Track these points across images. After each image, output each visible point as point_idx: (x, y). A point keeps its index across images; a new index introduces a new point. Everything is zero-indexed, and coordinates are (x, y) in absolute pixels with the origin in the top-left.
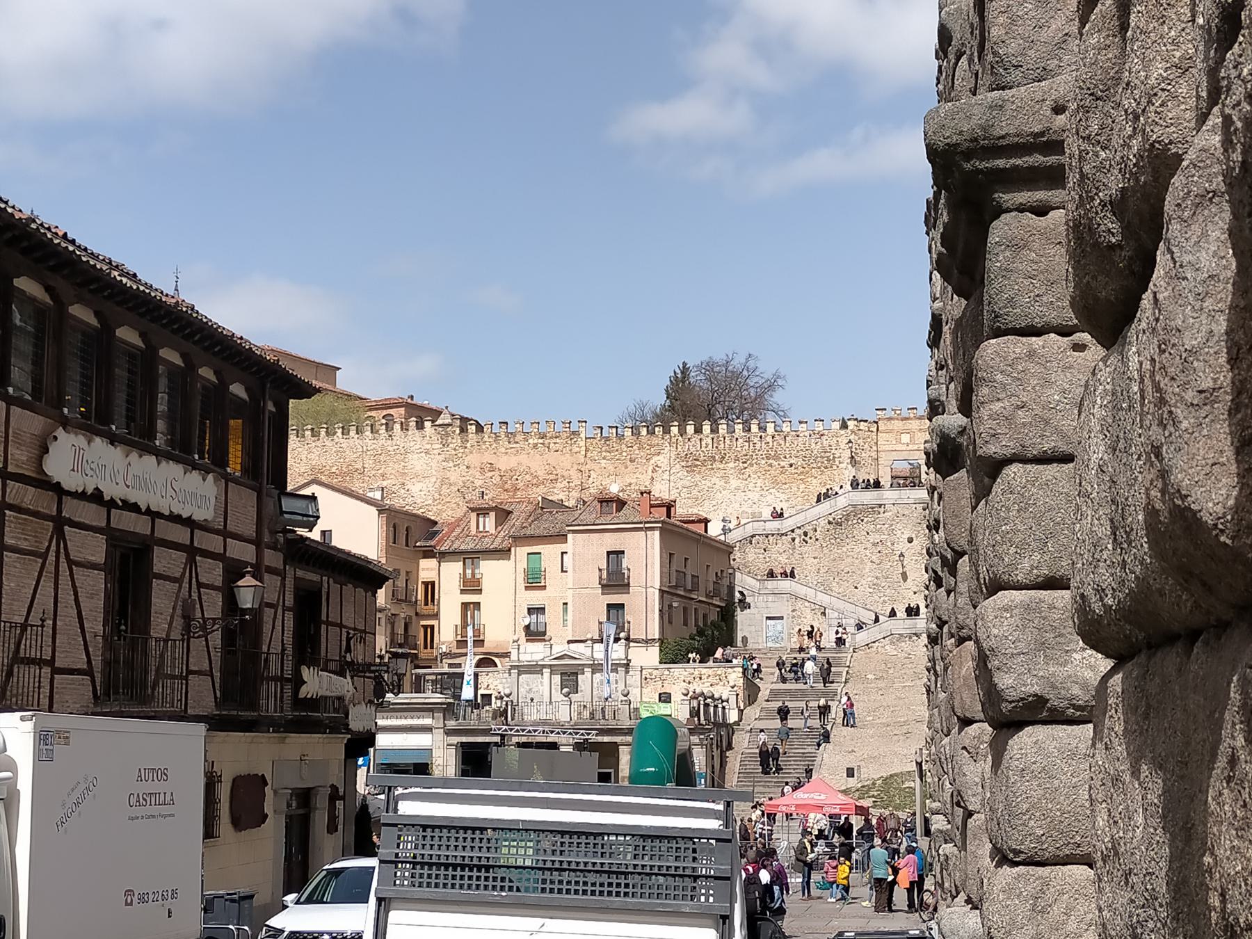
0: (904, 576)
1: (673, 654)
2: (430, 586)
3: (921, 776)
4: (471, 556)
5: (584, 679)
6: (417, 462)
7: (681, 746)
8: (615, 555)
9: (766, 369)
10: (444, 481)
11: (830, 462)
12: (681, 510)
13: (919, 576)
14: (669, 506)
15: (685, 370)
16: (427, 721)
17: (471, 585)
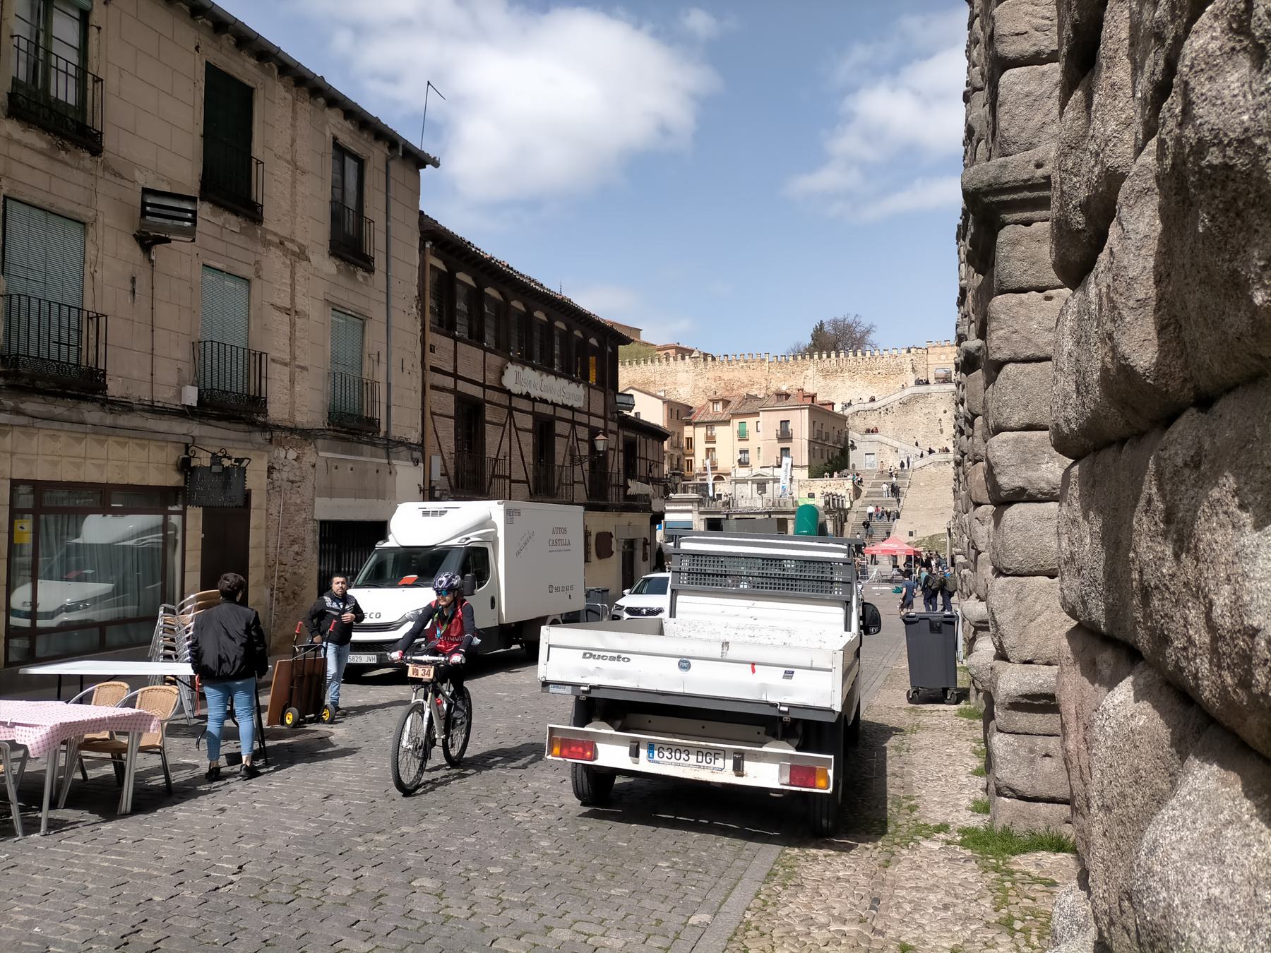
0: (942, 431)
1: (816, 473)
2: (690, 440)
3: (950, 535)
4: (710, 424)
5: (769, 486)
6: (682, 377)
7: (821, 520)
8: (785, 423)
9: (865, 322)
10: (696, 386)
11: (901, 371)
12: (820, 399)
13: (950, 430)
14: (813, 397)
15: (822, 324)
16: (690, 507)
17: (710, 439)
